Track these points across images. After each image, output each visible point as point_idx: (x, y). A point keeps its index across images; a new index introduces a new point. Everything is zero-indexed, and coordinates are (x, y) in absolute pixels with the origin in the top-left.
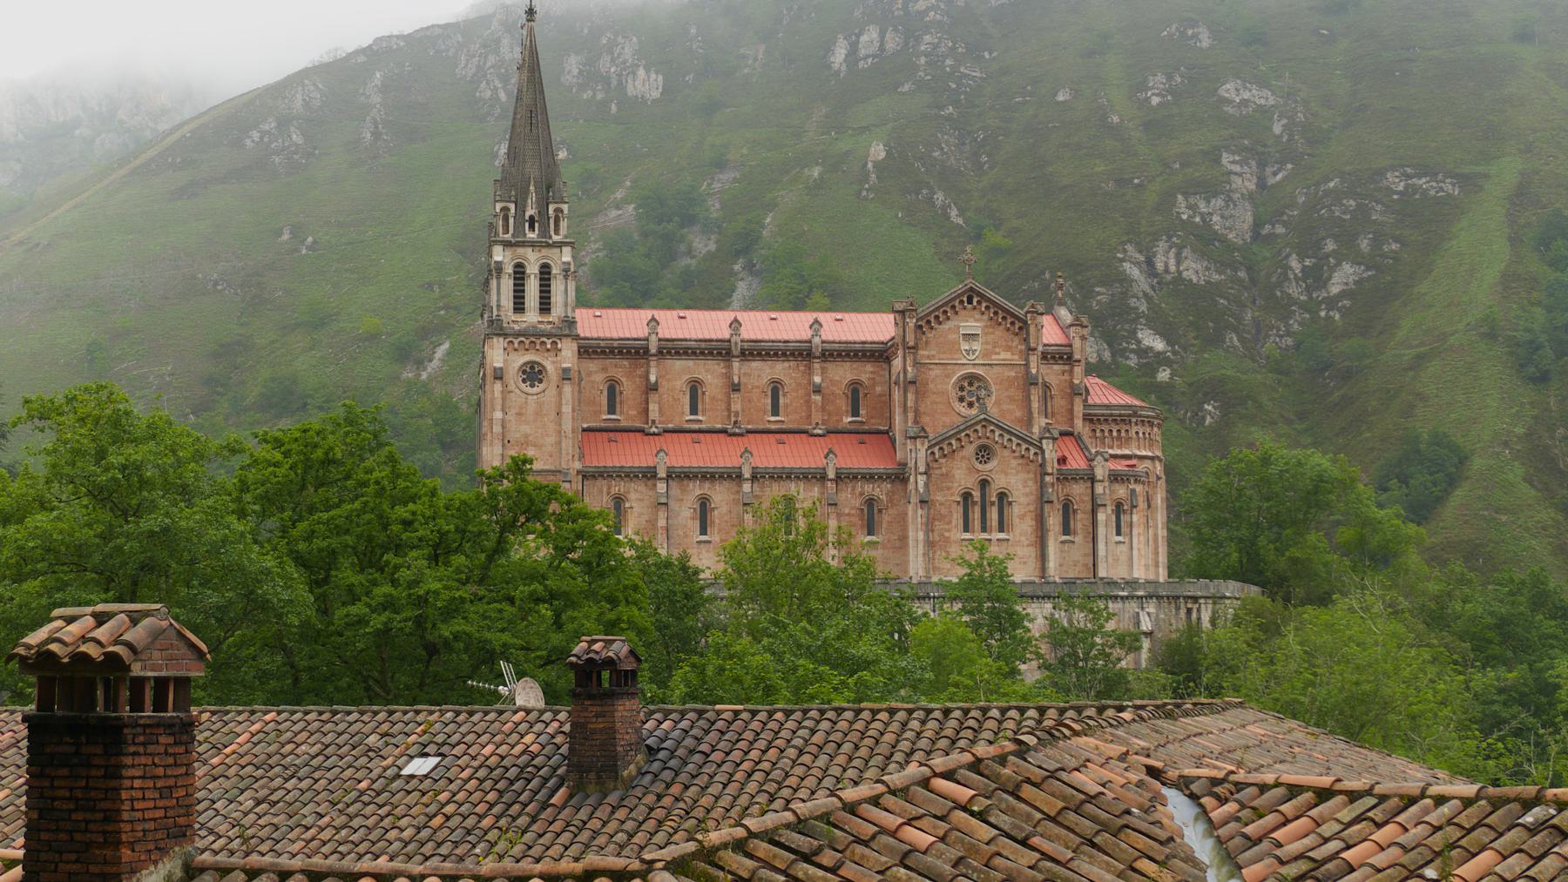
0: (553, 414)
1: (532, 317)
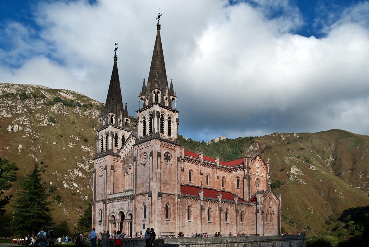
1: (166, 135)
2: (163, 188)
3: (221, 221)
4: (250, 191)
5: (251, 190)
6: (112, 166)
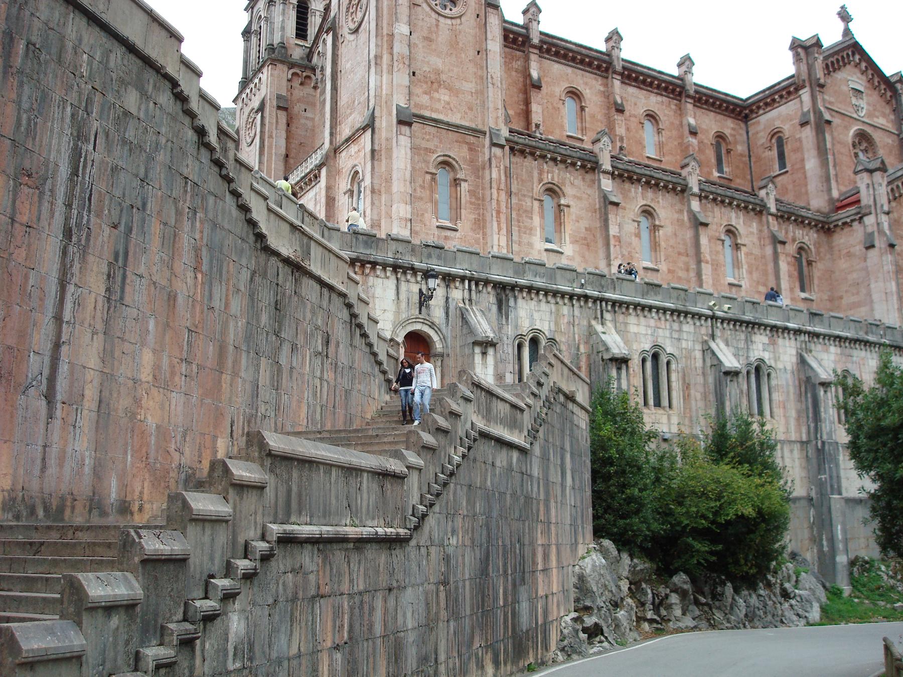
0: (472, 53)
2: (425, 99)
3: (703, 265)
4: (832, 172)
5: (835, 166)
6: (279, 97)
